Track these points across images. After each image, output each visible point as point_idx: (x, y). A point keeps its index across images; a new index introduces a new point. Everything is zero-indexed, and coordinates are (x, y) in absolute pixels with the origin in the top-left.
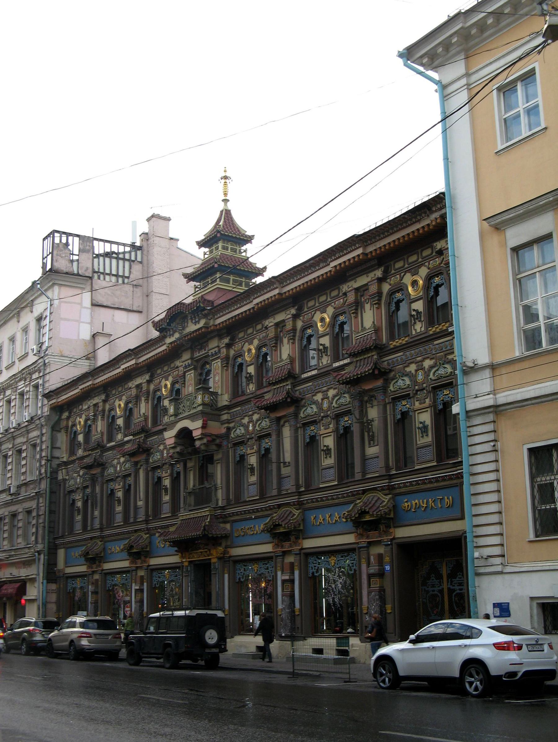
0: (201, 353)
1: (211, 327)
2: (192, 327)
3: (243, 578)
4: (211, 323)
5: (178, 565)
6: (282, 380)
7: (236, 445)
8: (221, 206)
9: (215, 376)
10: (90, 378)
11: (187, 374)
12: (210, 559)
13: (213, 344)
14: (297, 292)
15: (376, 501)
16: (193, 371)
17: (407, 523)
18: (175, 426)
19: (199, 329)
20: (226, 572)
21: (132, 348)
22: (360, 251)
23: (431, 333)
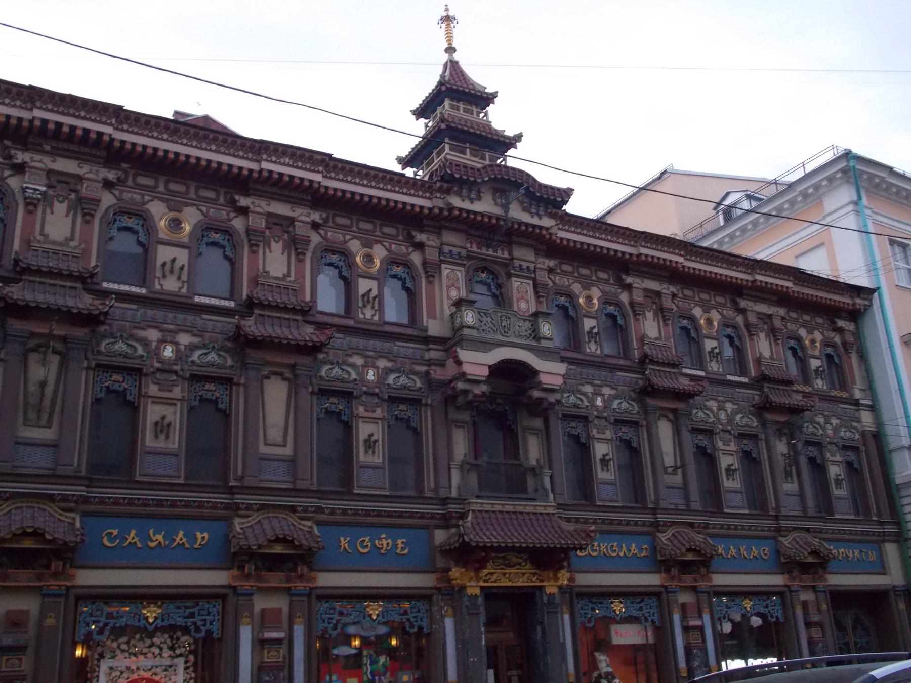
0: (484, 251)
1: (550, 234)
2: (517, 213)
3: (335, 628)
4: (554, 230)
5: (428, 592)
6: (658, 362)
7: (567, 417)
8: (445, 57)
9: (518, 300)
10: (114, 121)
11: (443, 266)
12: (544, 587)
13: (524, 255)
14: (710, 278)
15: (797, 543)
16: (462, 269)
17: (834, 571)
18: (491, 350)
19: (534, 226)
20: (565, 610)
21: (336, 155)
22: (790, 284)
23: (832, 394)
